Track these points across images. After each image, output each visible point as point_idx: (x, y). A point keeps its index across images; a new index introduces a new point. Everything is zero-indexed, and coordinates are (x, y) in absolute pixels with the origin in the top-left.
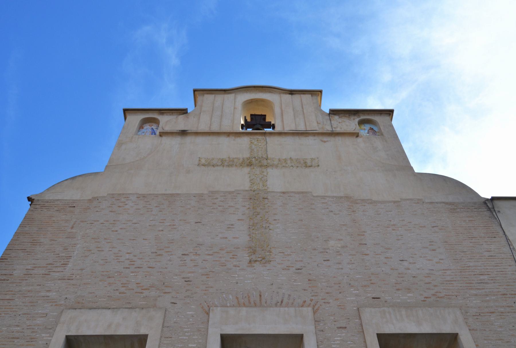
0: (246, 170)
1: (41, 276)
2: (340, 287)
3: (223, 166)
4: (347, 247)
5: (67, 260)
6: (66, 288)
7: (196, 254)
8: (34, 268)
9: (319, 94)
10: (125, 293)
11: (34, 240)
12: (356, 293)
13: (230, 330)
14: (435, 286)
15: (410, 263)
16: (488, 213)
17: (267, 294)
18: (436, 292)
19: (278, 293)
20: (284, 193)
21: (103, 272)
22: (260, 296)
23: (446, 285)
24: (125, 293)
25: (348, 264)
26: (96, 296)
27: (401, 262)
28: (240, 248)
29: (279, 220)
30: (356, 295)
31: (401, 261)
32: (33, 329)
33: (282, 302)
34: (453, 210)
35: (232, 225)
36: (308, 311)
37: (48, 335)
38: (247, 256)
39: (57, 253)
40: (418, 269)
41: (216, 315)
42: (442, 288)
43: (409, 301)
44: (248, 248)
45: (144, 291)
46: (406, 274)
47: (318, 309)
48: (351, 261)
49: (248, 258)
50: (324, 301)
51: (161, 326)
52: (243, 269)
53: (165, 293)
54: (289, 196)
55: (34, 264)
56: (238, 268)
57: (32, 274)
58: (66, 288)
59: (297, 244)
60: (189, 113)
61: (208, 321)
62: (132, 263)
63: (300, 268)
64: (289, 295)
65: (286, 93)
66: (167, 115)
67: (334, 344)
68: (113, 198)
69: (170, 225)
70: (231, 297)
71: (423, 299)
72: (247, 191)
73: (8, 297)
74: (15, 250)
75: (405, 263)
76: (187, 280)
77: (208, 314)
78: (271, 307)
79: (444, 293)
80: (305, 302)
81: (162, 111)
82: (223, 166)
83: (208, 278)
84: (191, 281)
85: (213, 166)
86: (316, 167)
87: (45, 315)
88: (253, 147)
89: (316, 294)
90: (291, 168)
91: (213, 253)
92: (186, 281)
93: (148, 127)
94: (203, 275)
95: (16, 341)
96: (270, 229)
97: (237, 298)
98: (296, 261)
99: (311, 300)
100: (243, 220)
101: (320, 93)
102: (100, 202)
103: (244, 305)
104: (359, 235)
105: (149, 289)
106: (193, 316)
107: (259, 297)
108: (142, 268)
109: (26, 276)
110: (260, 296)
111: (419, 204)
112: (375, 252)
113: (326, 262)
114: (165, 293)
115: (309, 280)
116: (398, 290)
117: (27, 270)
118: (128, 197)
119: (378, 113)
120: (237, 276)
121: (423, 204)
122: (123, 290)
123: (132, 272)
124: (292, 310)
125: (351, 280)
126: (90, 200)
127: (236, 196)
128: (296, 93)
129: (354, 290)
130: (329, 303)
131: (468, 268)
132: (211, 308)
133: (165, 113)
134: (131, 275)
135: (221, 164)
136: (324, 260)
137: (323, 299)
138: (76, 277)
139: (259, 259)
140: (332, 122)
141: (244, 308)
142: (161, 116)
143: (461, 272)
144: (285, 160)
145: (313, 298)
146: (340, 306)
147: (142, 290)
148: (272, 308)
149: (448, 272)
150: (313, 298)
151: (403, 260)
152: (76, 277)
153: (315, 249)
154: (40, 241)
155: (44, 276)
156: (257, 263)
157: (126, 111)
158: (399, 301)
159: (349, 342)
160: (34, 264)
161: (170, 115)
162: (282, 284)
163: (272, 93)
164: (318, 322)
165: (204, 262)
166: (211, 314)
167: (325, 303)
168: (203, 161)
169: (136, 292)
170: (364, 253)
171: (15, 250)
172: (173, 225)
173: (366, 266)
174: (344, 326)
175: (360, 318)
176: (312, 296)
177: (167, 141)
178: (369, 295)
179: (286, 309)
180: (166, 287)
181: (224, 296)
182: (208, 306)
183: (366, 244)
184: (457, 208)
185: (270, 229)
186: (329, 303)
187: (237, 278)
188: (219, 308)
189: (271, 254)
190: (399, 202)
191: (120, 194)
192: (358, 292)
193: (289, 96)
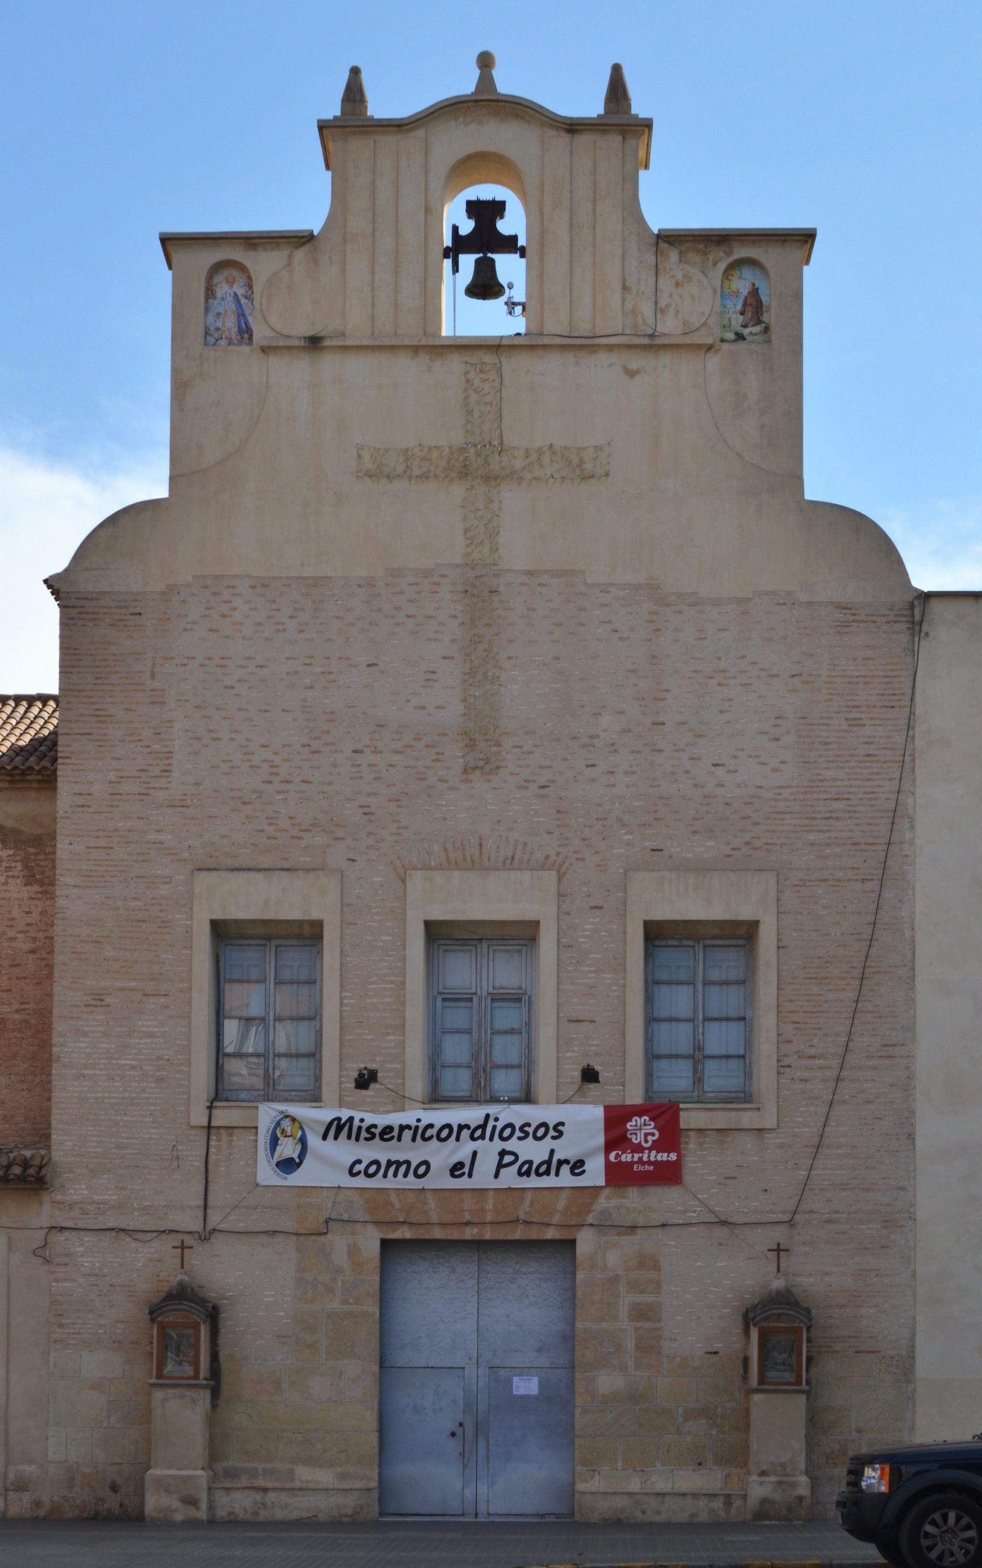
0: (457, 491)
1: (137, 797)
2: (604, 826)
3: (410, 478)
4: (630, 731)
5: (167, 762)
6: (184, 825)
7: (377, 751)
8: (120, 780)
9: (644, 131)
10: (276, 838)
11: (97, 710)
12: (629, 839)
13: (437, 914)
14: (757, 824)
15: (729, 771)
16: (904, 638)
17: (491, 841)
18: (753, 838)
19: (507, 839)
20: (530, 573)
21: (231, 790)
22: (481, 845)
23: (773, 822)
24: (276, 838)
25: (626, 773)
26: (234, 844)
27: (713, 768)
28: (448, 734)
29: (517, 658)
30: (629, 844)
31: (714, 765)
32: (160, 905)
33: (513, 858)
34: (845, 626)
35: (433, 672)
36: (549, 877)
37: (184, 916)
38: (460, 754)
39: (147, 744)
40: (739, 785)
41: (416, 883)
42: (766, 828)
43: (706, 856)
44: (462, 734)
45: (304, 834)
46: (715, 797)
47: (565, 873)
48: (631, 766)
49: (462, 760)
50: (576, 856)
51: (339, 905)
52: (452, 789)
53: (336, 839)
54: (539, 585)
55: (118, 770)
56: (447, 785)
57: (120, 794)
58: (184, 825)
59: (545, 724)
60: (318, 235)
61: (405, 896)
62: (274, 770)
63: (546, 784)
64: (525, 844)
65: (557, 128)
66: (265, 250)
67: (583, 937)
68: (206, 587)
69: (323, 673)
70: (436, 848)
71: (728, 852)
72: (458, 566)
73: (103, 843)
74: (75, 734)
75: (720, 771)
76: (366, 810)
77: (404, 881)
78: (497, 869)
79: (765, 840)
80: (547, 857)
81: (252, 241)
82: (410, 478)
83: (399, 806)
84: (373, 814)
85: (388, 477)
86: (603, 479)
87: (168, 880)
88: (474, 397)
89: (566, 842)
90: (551, 480)
91: (404, 746)
92: (365, 814)
93: (224, 291)
94: (390, 801)
95: (144, 927)
96: (500, 685)
97: (446, 850)
98: (541, 767)
99: (558, 854)
100: (453, 658)
101: (646, 130)
102: (183, 601)
103: (458, 868)
104: (655, 699)
105: (310, 831)
106: (382, 886)
107: (478, 847)
108: (291, 782)
109: (114, 797)
110: (481, 845)
111: (785, 607)
112: (675, 745)
113: (590, 769)
114: (336, 839)
115: (558, 812)
116: (694, 832)
117: (112, 785)
118: (233, 587)
119: (777, 241)
120: (444, 803)
121: (792, 609)
122: (270, 830)
123: (279, 792)
124: (527, 875)
125: (624, 812)
126: (163, 593)
127: (439, 584)
128: (583, 130)
129: (626, 834)
130: (583, 860)
131: (820, 784)
132: (408, 872)
133: (261, 244)
134: (278, 797)
135: (405, 472)
136: (588, 766)
137: (575, 852)
138: (192, 801)
139: (481, 763)
140: (661, 280)
141: (457, 874)
142: (251, 254)
143: (806, 793)
144: (540, 451)
145: (561, 849)
146: (600, 865)
147: (301, 831)
148: (497, 873)
149: (786, 793)
150: (561, 849)
151: (719, 763)
152: (192, 801)
153: (574, 738)
154: (107, 713)
155: (142, 797)
156: (478, 772)
157: (167, 242)
158: (690, 856)
159: (603, 934)
160: (118, 770)
161: (273, 249)
162: (515, 821)
163: (522, 118)
164: (565, 896)
165: (390, 769)
166: (408, 884)
167: (577, 859)
168: (368, 464)
169: (293, 837)
170: (656, 748)
171: (75, 734)
172: (329, 673)
173: (654, 780)
174: (600, 905)
175: (625, 891)
176: (560, 846)
177: (276, 363)
178: (647, 844)
179: (518, 873)
180: (336, 825)
181: (426, 846)
182: (403, 867)
183: (663, 724)
184: (853, 621)
185: (500, 685)
186: (583, 860)
187: (444, 808)
188: (419, 872)
189: (501, 749)
190: (749, 599)
191: (216, 577)
192: (631, 837)
193: (565, 138)
